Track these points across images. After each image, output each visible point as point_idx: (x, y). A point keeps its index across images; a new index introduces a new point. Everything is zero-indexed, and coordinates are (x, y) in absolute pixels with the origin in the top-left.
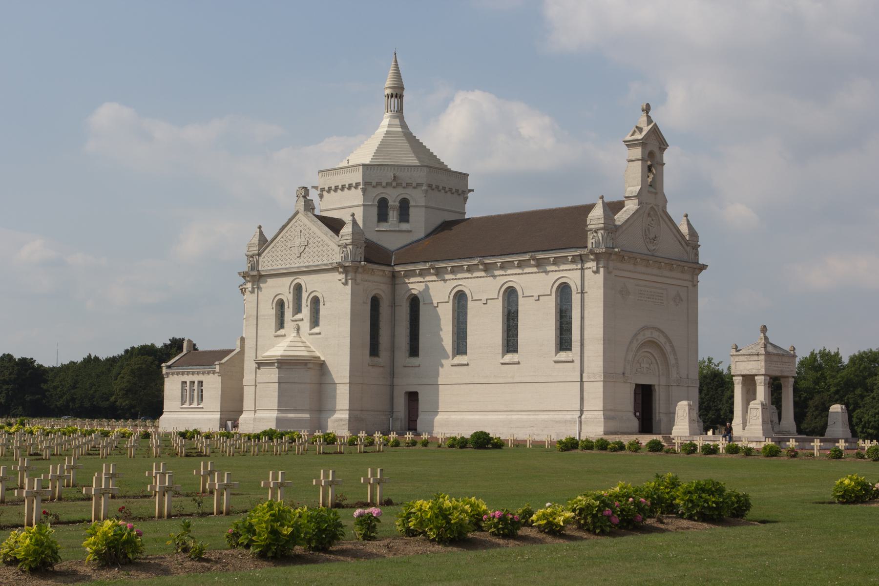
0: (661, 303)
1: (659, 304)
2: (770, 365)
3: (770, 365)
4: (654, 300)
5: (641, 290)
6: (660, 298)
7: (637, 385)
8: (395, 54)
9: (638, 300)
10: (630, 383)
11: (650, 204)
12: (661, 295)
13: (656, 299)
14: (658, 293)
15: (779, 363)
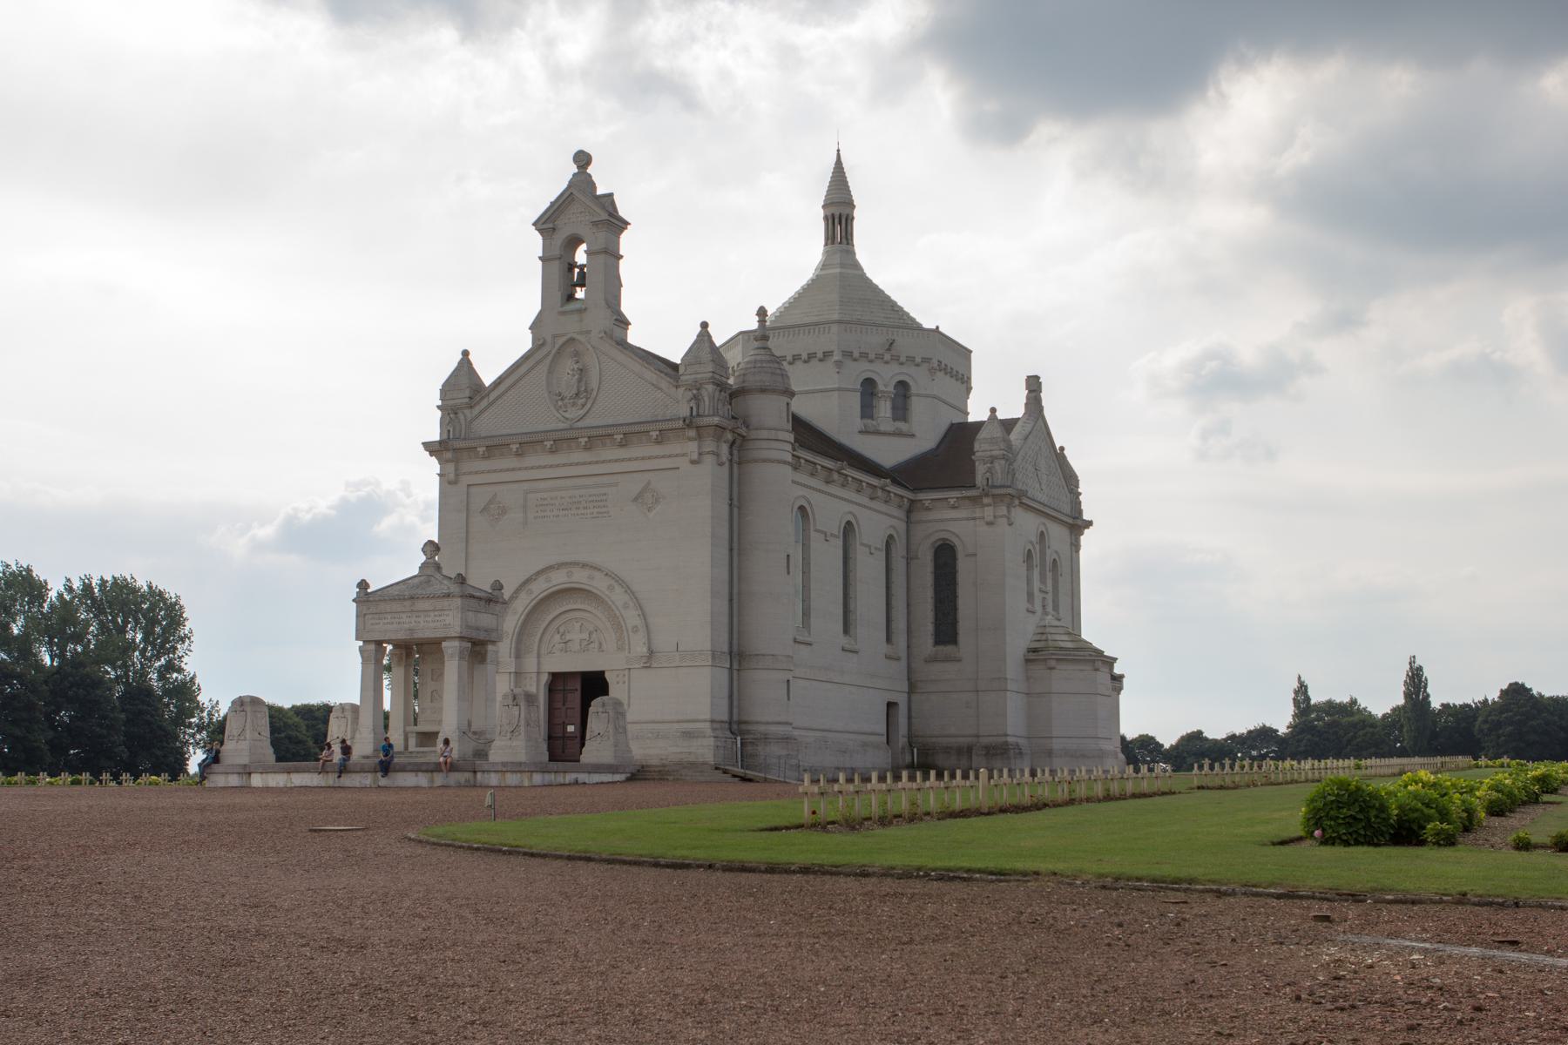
0: (598, 513)
1: (595, 515)
2: (377, 621)
3: (377, 621)
4: (579, 512)
5: (545, 499)
6: (595, 504)
7: (549, 673)
8: (838, 151)
9: (536, 518)
10: (510, 673)
11: (563, 335)
12: (604, 498)
13: (585, 508)
14: (590, 496)
15: (404, 616)
